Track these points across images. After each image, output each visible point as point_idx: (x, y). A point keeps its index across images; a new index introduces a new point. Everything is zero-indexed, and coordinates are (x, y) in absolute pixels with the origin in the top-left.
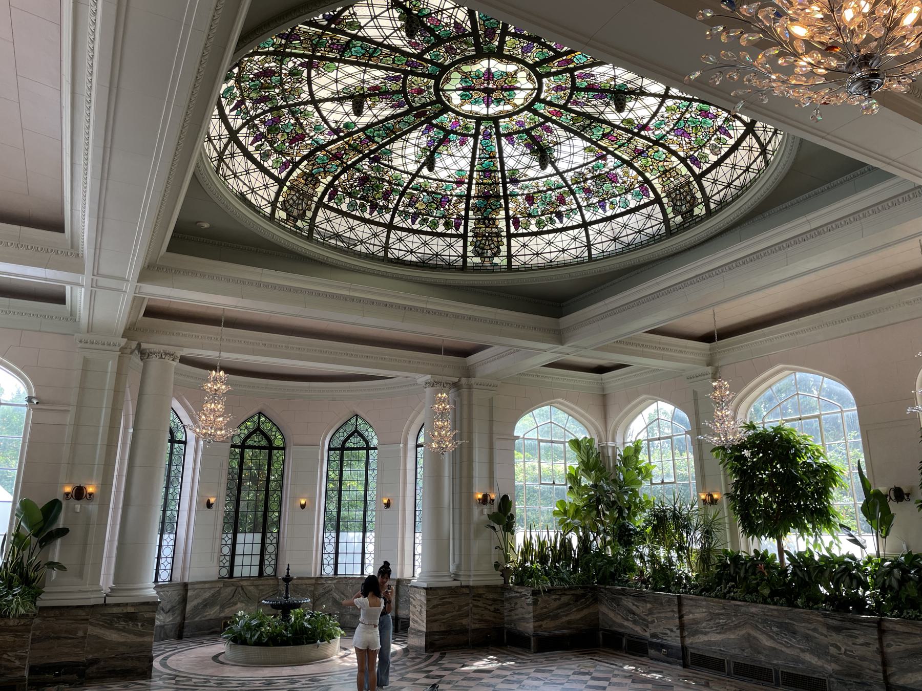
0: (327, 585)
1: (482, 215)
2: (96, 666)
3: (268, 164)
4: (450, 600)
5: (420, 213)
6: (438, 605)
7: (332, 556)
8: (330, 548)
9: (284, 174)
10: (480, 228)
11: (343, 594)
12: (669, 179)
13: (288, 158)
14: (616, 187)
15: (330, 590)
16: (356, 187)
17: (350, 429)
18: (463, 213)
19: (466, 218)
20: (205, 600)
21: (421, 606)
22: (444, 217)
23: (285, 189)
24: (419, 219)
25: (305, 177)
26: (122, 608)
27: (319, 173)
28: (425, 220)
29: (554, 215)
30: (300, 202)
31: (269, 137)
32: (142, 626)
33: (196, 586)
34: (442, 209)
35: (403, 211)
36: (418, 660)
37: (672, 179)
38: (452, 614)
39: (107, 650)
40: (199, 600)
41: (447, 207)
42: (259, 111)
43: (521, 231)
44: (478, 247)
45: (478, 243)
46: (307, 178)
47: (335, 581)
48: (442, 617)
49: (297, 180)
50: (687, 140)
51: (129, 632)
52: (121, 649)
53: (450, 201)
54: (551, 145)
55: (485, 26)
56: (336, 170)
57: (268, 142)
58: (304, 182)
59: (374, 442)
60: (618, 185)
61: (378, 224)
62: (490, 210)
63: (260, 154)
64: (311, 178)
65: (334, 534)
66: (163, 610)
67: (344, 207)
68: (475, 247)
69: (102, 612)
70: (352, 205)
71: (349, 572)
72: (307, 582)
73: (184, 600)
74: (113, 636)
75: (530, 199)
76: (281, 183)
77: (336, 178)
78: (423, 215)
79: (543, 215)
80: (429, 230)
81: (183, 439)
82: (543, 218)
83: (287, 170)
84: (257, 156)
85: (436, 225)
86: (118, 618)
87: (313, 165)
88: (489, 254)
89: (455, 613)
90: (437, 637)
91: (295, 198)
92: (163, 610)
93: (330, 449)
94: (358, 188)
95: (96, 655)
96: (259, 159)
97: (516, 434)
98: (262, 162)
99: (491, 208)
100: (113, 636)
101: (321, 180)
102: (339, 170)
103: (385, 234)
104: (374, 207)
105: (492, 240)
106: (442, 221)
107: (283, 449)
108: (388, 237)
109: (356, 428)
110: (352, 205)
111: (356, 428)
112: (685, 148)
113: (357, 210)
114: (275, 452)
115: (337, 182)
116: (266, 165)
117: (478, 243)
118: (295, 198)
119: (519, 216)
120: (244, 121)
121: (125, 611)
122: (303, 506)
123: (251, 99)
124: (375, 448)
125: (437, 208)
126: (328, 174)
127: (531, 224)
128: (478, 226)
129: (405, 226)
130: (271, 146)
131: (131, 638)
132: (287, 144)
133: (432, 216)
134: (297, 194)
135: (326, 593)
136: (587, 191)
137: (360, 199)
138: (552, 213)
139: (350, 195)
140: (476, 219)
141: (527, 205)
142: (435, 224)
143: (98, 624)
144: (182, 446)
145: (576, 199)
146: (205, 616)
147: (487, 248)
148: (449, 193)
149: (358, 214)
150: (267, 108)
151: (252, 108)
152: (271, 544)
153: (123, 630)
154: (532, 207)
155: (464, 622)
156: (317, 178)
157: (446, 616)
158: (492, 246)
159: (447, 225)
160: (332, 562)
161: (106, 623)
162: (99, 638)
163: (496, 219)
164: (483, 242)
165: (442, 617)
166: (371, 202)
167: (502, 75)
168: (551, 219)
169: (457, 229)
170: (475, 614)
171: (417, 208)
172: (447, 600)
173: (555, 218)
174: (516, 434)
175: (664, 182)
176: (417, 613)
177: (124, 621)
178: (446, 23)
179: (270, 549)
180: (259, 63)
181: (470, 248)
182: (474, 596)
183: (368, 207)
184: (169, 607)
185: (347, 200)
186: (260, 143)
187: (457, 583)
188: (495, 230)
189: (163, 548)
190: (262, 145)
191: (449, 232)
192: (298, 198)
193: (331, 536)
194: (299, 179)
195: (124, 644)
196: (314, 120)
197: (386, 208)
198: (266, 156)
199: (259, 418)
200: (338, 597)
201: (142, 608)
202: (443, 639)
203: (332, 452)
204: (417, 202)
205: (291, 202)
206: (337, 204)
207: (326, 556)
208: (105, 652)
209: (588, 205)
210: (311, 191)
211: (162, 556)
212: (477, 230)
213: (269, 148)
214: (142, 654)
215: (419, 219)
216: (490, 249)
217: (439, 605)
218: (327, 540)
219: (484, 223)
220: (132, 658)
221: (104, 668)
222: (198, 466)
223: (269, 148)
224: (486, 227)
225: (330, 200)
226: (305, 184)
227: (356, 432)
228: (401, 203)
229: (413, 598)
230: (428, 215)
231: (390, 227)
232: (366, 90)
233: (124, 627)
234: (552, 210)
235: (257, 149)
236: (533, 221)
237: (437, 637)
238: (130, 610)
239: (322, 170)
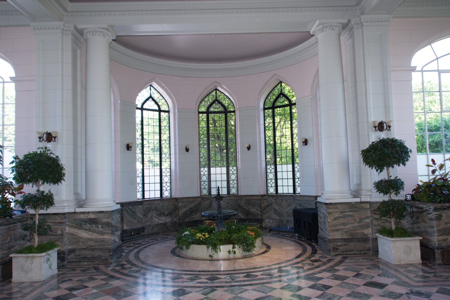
0: (269, 200)
2: (73, 254)
4: (351, 213)
6: (338, 218)
7: (273, 181)
8: (271, 176)
11: (280, 206)
15: (271, 204)
17: (276, 92)
20: (191, 208)
21: (324, 218)
26: (86, 215)
32: (102, 227)
33: (184, 200)
36: (316, 264)
38: (353, 225)
39: (80, 243)
40: (187, 209)
47: (274, 198)
48: (343, 227)
51: (94, 231)
59: (294, 100)
65: (273, 167)
66: (163, 214)
69: (74, 218)
71: (286, 191)
72: (256, 198)
73: (176, 208)
74: (84, 234)
81: (167, 109)
86: (85, 222)
89: (356, 224)
90: (339, 244)
92: (163, 214)
93: (265, 109)
95: (73, 246)
97: (413, 64)
100: (84, 234)
107: (234, 112)
109: (281, 91)
111: (281, 91)
114: (229, 114)
121: (89, 217)
122: (249, 148)
124: (295, 104)
131: (95, 236)
135: (269, 205)
143: (73, 226)
144: (167, 114)
146: (192, 218)
152: (233, 174)
153: (89, 230)
155: (366, 231)
157: (347, 227)
160: (274, 185)
161: (77, 225)
162: (74, 235)
165: (343, 227)
170: (376, 226)
172: (347, 213)
174: (413, 64)
176: (323, 223)
177: (89, 224)
179: (233, 177)
182: (373, 211)
184: (167, 212)
187: (358, 200)
189: (163, 177)
193: (271, 168)
195: (91, 240)
199: (216, 93)
200: (277, 208)
201: (102, 215)
202: (345, 245)
203: (266, 111)
207: (269, 181)
208: (79, 245)
211: (163, 182)
214: (104, 247)
217: (341, 217)
218: (269, 171)
220: (97, 249)
221: (79, 255)
227: (282, 94)
229: (319, 212)
233: (90, 228)
237: (339, 244)
238: (92, 216)
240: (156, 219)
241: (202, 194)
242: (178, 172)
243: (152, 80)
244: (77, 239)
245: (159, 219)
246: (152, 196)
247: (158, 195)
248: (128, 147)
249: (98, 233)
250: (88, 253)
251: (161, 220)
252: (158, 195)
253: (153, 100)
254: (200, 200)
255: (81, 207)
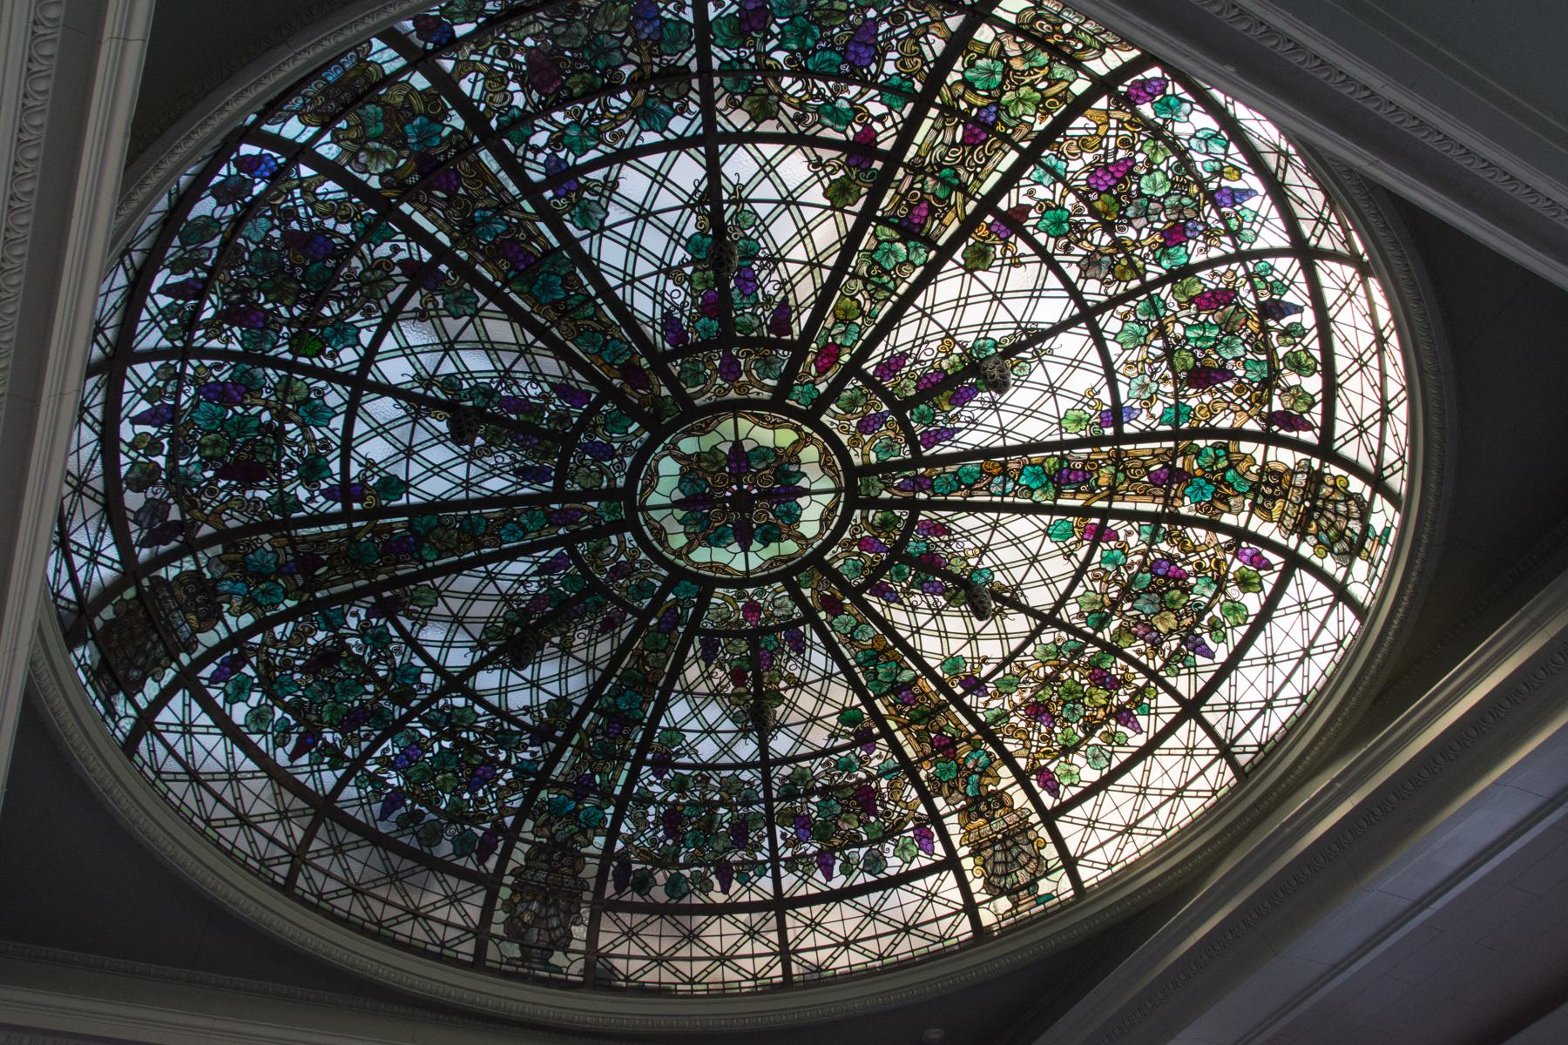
1: (1244, 494)
3: (894, 865)
5: (1190, 629)
9: (939, 849)
10: (1284, 513)
12: (1071, 36)
13: (911, 825)
14: (1149, 162)
16: (1051, 731)
18: (1223, 538)
19: (1240, 534)
22: (1220, 583)
23: (968, 863)
24: (1206, 637)
25: (974, 814)
27: (980, 785)
28: (1214, 627)
29: (1271, 323)
30: (1015, 851)
31: (837, 842)
34: (1192, 580)
35: (1166, 664)
37: (1067, 28)
41: (1188, 568)
42: (766, 843)
43: (1316, 415)
44: (1333, 544)
45: (1324, 537)
46: (977, 810)
49: (969, 832)
50: (884, 27)
53: (1170, 559)
54: (957, 350)
55: (543, 528)
56: (989, 754)
57: (847, 847)
58: (981, 821)
60: (1140, 158)
61: (1170, 729)
62: (1230, 475)
63: (862, 871)
64: (983, 804)
67: (1091, 775)
68: (1332, 551)
70: (1095, 758)
75: (1203, 377)
76: (951, 862)
77: (1008, 759)
78: (1196, 624)
79: (1271, 352)
80: (1243, 630)
82: (1281, 352)
83: (936, 838)
84: (862, 879)
85: (1236, 608)
87: (952, 789)
88: (1356, 526)
91: (999, 857)
94: (1057, 730)
96: (870, 878)
98: (882, 876)
99: (1225, 470)
101: (1000, 787)
102: (990, 749)
103: (1201, 733)
104: (1123, 715)
105: (1327, 499)
106: (1233, 591)
108: (1210, 730)
110: (1095, 758)
112: (927, 19)
113: (1112, 753)
115: (1022, 763)
116: (892, 872)
117: (1324, 537)
118: (999, 857)
119: (1265, 409)
120: (769, 873)
123: (727, 850)
125: (1187, 590)
126: (991, 771)
127: (1298, 387)
128: (1276, 514)
129: (1207, 677)
130: (861, 844)
132: (872, 819)
133: (1209, 608)
134: (997, 847)
136: (1175, 235)
137: (1090, 735)
138: (1265, 329)
139: (1068, 750)
140: (1251, 512)
141: (1229, 384)
142: (1235, 609)
145: (1210, 264)
147: (1342, 524)
148: (1139, 557)
149: (1123, 757)
150: (765, 830)
151: (752, 852)
154: (1240, 373)
156: (990, 794)
158: (1342, 508)
159: (1245, 583)
163: (1262, 467)
164: (1323, 523)
166: (1109, 716)
167: (693, 481)
168: (1286, 333)
169: (1269, 566)
171: (1171, 632)
173: (1285, 322)
175: (1086, 48)
178: (541, 587)
180: (642, 828)
181: (1329, 565)
183: (1120, 728)
185: (1078, 759)
186: (838, 863)
188: (1300, 480)
190: (847, 860)
191: (1268, 588)
192: (1007, 850)
194: (970, 826)
196: (820, 769)
197: (1141, 691)
198: (875, 863)
204: (1151, 628)
205: (1000, 869)
206: (1072, 784)
209: (1234, 234)
210: (1011, 819)
212: (1288, 522)
213: (863, 851)
215: (1206, 637)
216: (1348, 518)
219: (1273, 498)
223: (863, 851)
224: (1285, 496)
225: (1054, 792)
226: (989, 821)
228: (1143, 659)
230: (1201, 615)
231: (1190, 709)
232: (742, 690)
234: (1253, 326)
235: (847, 870)
236: (1292, 379)
239: (975, 777)
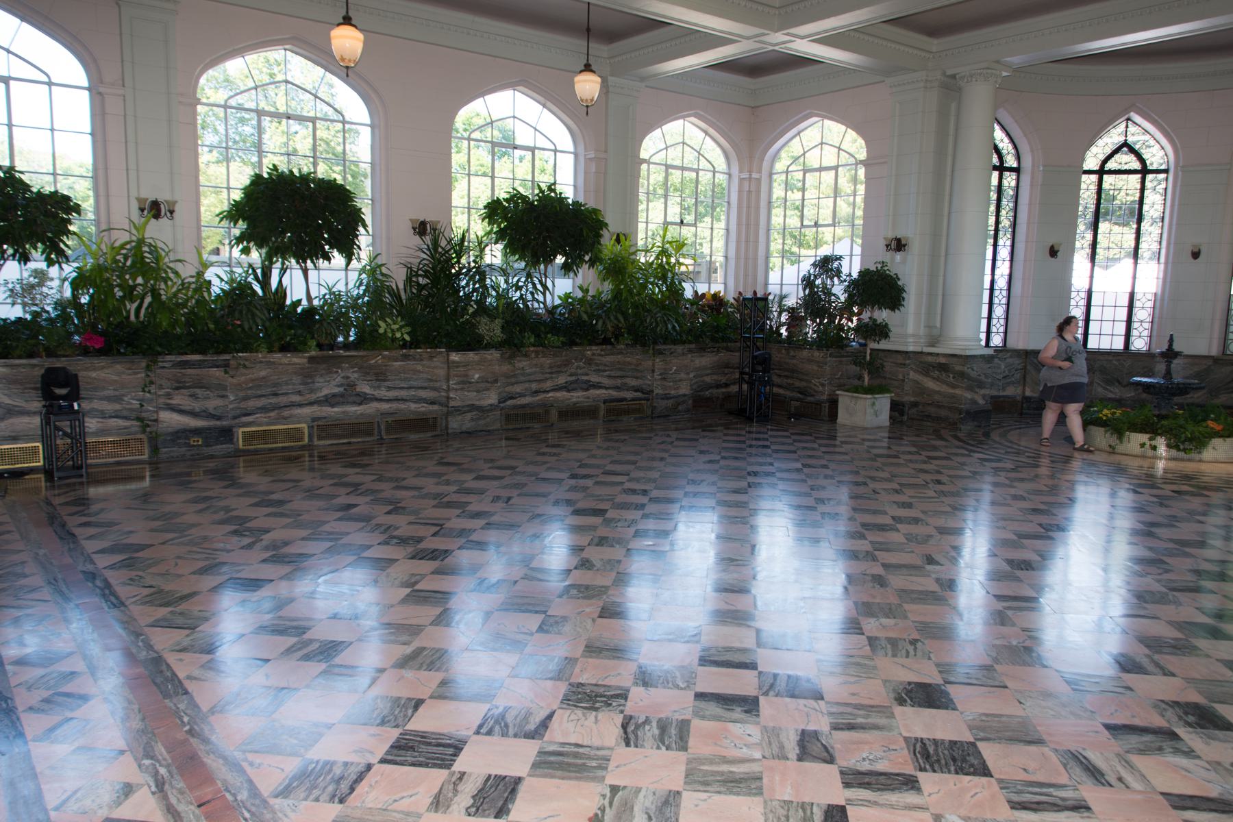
52: (937, 397)
74: (930, 384)
86: (933, 367)
100: (930, 384)
131: (944, 388)
153: (937, 379)
189: (1135, 310)
195: (938, 392)
201: (954, 360)
211: (1134, 319)
222: (1177, 203)
238: (943, 360)
240: (1100, 390)
241: (1228, 353)
242: (1166, 302)
243: (1127, 111)
244: (922, 391)
245: (1107, 389)
246: (1105, 344)
247: (1119, 344)
248: (1053, 252)
249: (948, 384)
250: (932, 410)
251: (1111, 392)
252: (1119, 344)
253: (1132, 150)
254: (1210, 362)
255: (933, 346)
